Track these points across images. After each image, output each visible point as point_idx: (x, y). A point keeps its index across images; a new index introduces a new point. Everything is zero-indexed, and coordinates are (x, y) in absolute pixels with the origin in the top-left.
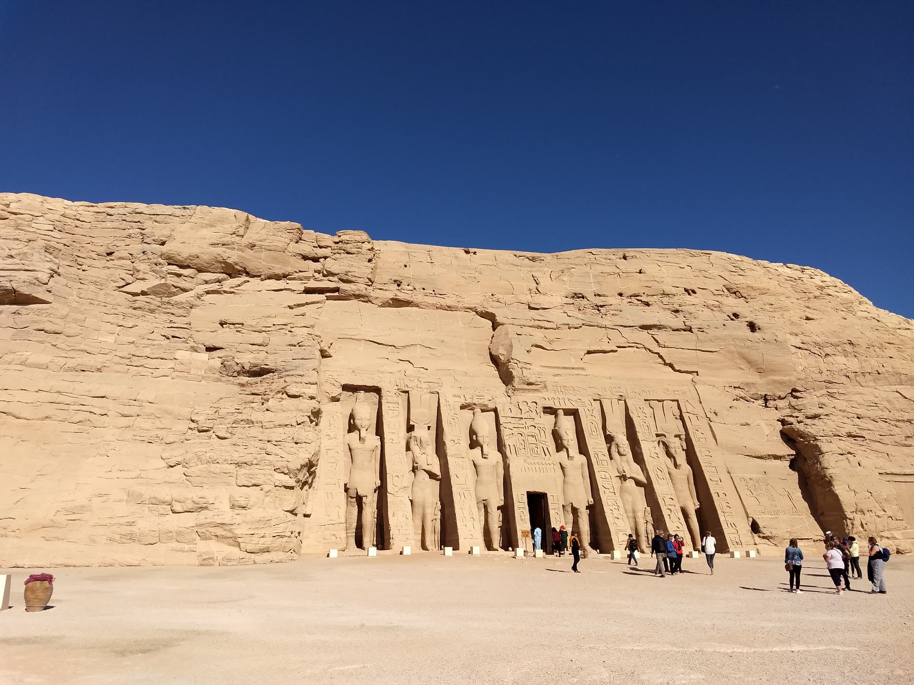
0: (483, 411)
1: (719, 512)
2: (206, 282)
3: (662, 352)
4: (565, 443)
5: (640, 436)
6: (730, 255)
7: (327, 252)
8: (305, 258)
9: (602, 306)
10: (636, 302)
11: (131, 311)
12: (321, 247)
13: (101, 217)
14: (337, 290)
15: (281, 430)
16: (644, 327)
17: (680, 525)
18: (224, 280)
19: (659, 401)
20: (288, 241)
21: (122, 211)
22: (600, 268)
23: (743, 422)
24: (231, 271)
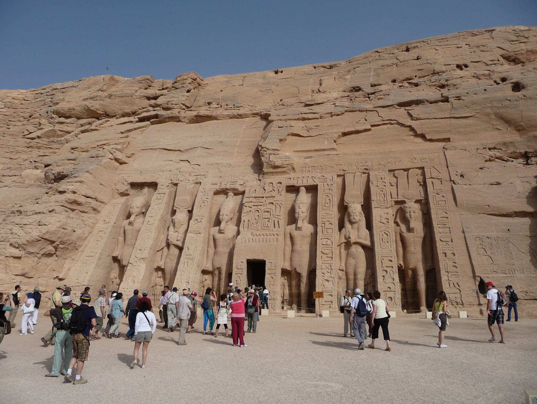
0: (235, 194)
1: (443, 273)
2: (82, 125)
3: (414, 124)
4: (296, 215)
5: (374, 204)
6: (516, 27)
7: (165, 91)
8: (149, 98)
9: (372, 94)
10: (407, 85)
11: (26, 149)
12: (163, 89)
13: (37, 96)
14: (156, 116)
15: (35, 216)
16: (401, 105)
17: (391, 286)
18: (94, 122)
19: (405, 170)
20: (136, 89)
21: (47, 90)
22: (381, 62)
23: (494, 181)
24: (95, 115)
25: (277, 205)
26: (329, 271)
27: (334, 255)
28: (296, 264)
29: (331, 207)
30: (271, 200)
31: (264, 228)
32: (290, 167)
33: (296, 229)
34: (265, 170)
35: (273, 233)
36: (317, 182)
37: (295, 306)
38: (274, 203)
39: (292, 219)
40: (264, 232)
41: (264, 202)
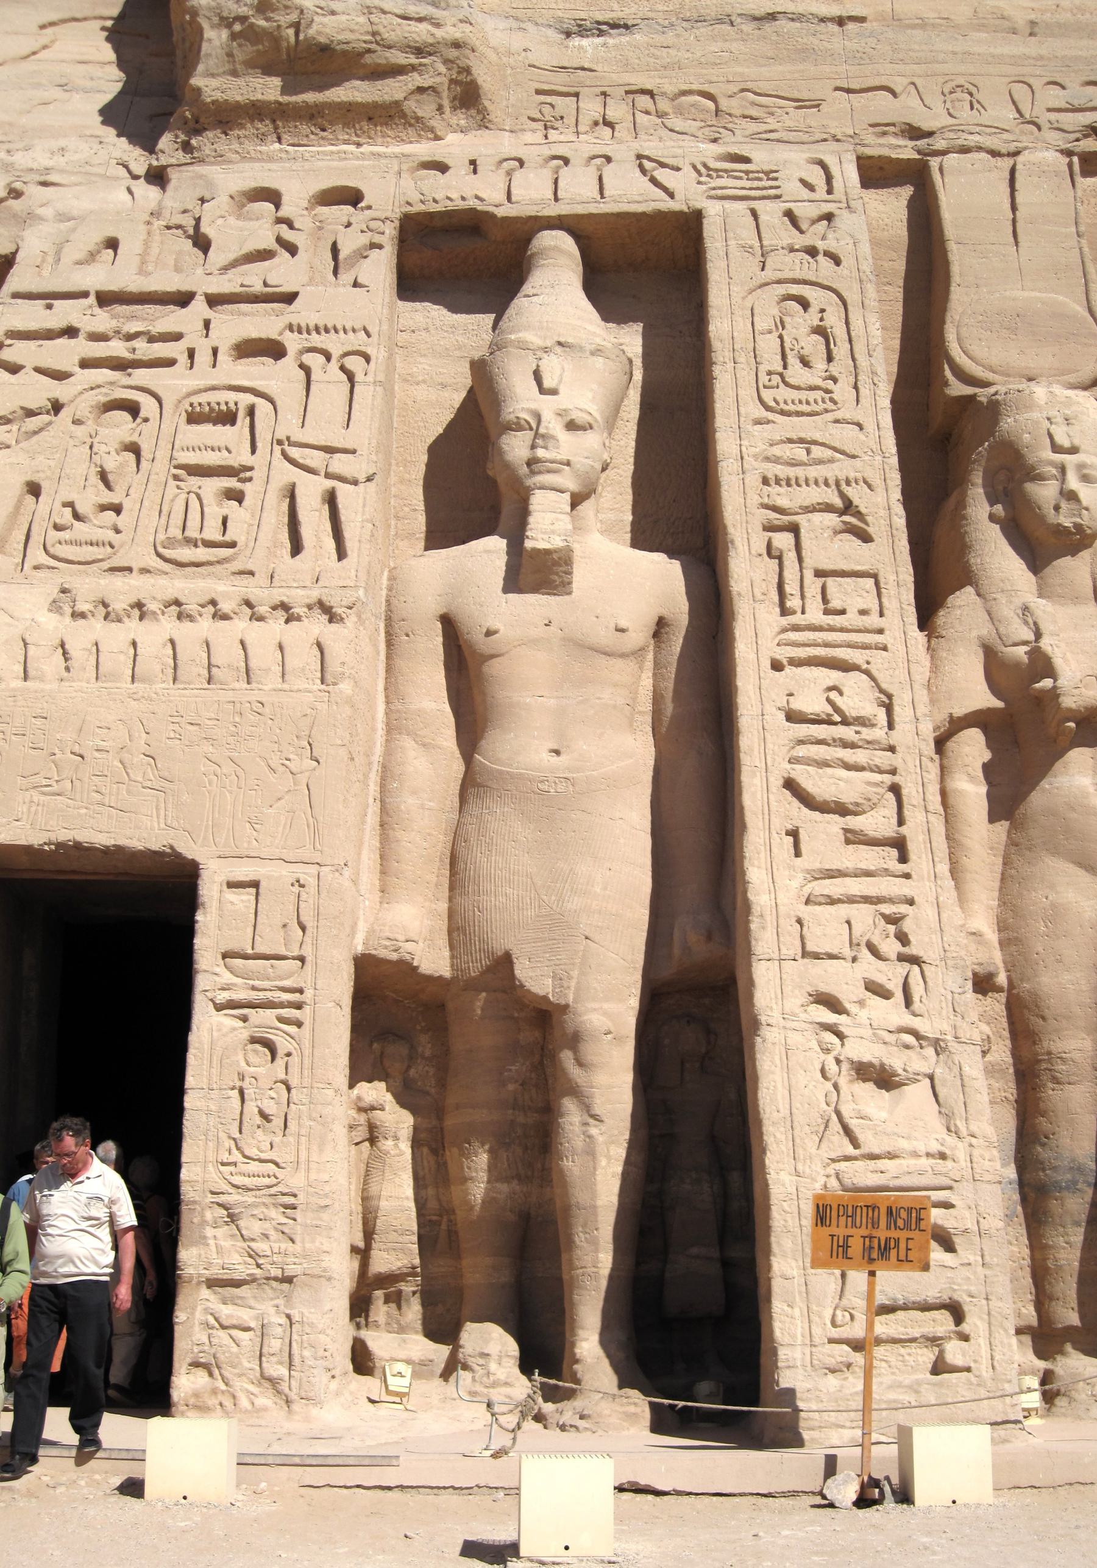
4: (516, 448)
25: (315, 361)
26: (891, 975)
27: (915, 817)
28: (510, 921)
29: (843, 391)
30: (261, 323)
31: (186, 554)
32: (436, 74)
33: (514, 582)
34: (211, 83)
35: (279, 595)
36: (687, 192)
37: (492, 1344)
38: (292, 343)
39: (471, 483)
40: (189, 587)
41: (194, 338)
